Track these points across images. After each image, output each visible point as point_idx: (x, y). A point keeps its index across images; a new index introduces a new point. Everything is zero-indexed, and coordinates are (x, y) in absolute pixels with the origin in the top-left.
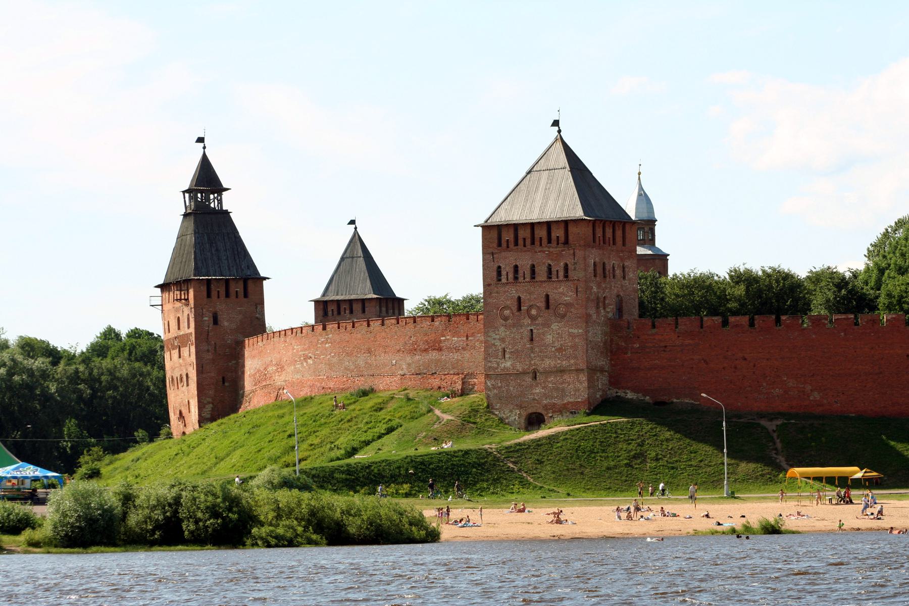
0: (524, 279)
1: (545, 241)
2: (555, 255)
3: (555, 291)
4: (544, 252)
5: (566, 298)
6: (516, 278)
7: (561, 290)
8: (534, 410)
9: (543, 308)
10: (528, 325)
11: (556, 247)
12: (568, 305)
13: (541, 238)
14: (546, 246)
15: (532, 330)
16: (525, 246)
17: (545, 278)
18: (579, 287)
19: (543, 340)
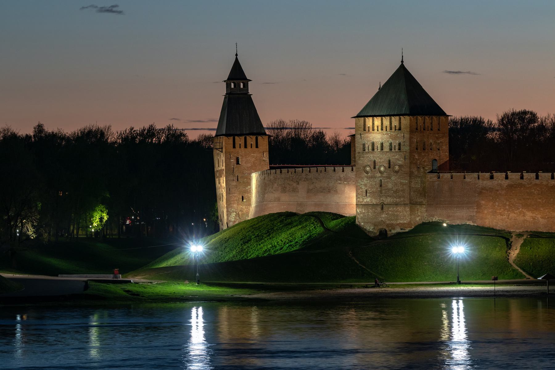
0: (377, 150)
2: (394, 137)
3: (394, 158)
4: (388, 134)
5: (399, 162)
7: (397, 157)
10: (379, 177)
11: (394, 132)
13: (386, 126)
18: (406, 156)
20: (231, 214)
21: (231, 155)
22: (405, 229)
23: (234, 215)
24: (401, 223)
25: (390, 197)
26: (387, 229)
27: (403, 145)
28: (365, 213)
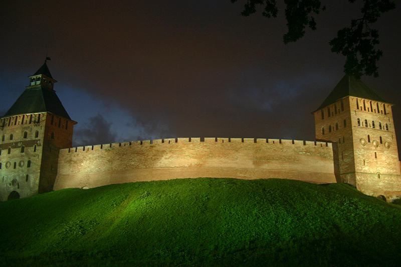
6: (367, 126)
7: (386, 135)
17: (379, 128)
26: (385, 196)
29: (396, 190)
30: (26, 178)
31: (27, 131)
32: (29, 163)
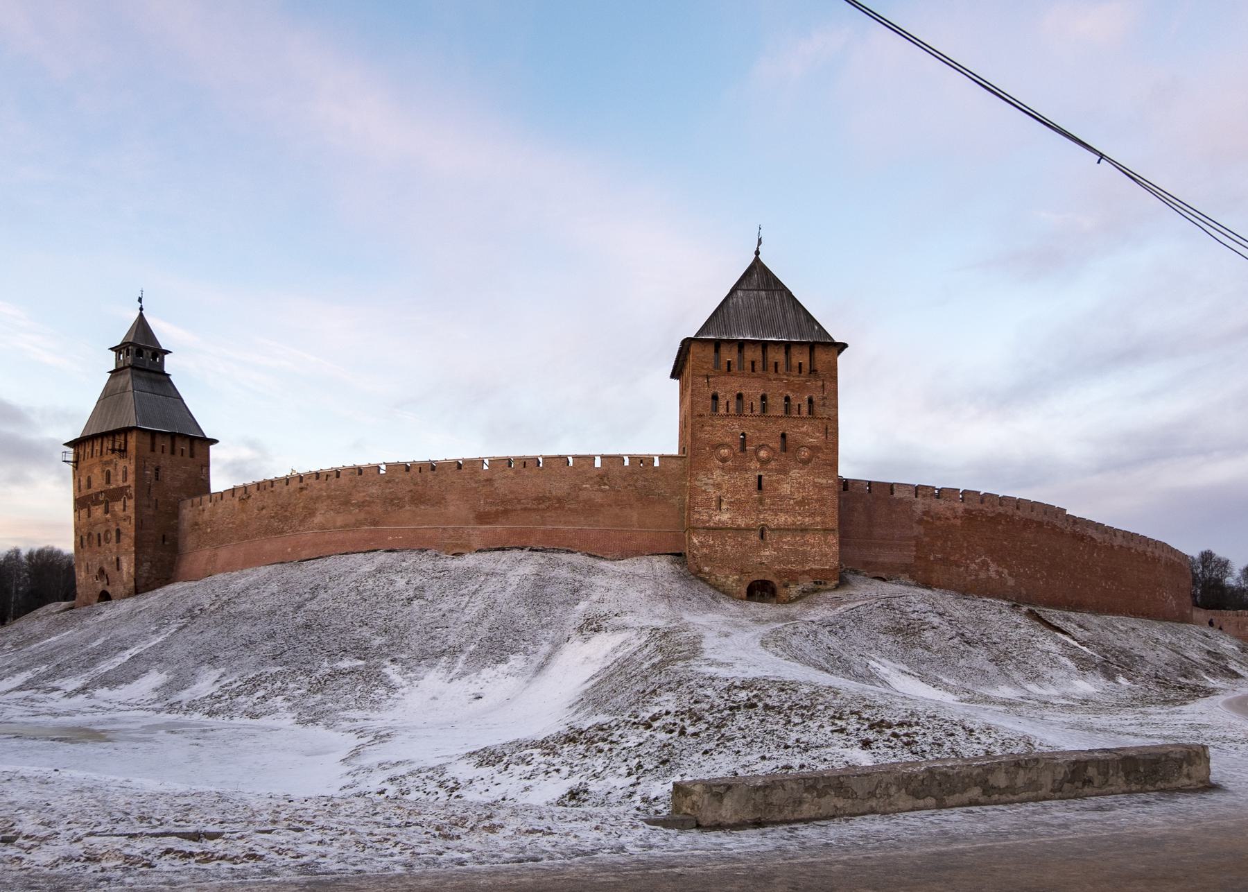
0: (752, 411)
1: (782, 368)
2: (797, 386)
4: (781, 380)
7: (804, 429)
8: (761, 577)
9: (779, 450)
10: (756, 469)
11: (799, 377)
12: (814, 449)
13: (776, 363)
14: (785, 374)
15: (760, 477)
16: (753, 370)
19: (777, 489)
20: (142, 565)
21: (147, 463)
22: (825, 584)
23: (146, 566)
24: (815, 570)
25: (787, 513)
26: (776, 581)
27: (821, 403)
28: (713, 546)
29: (814, 567)
30: (115, 564)
31: (110, 469)
32: (118, 532)
